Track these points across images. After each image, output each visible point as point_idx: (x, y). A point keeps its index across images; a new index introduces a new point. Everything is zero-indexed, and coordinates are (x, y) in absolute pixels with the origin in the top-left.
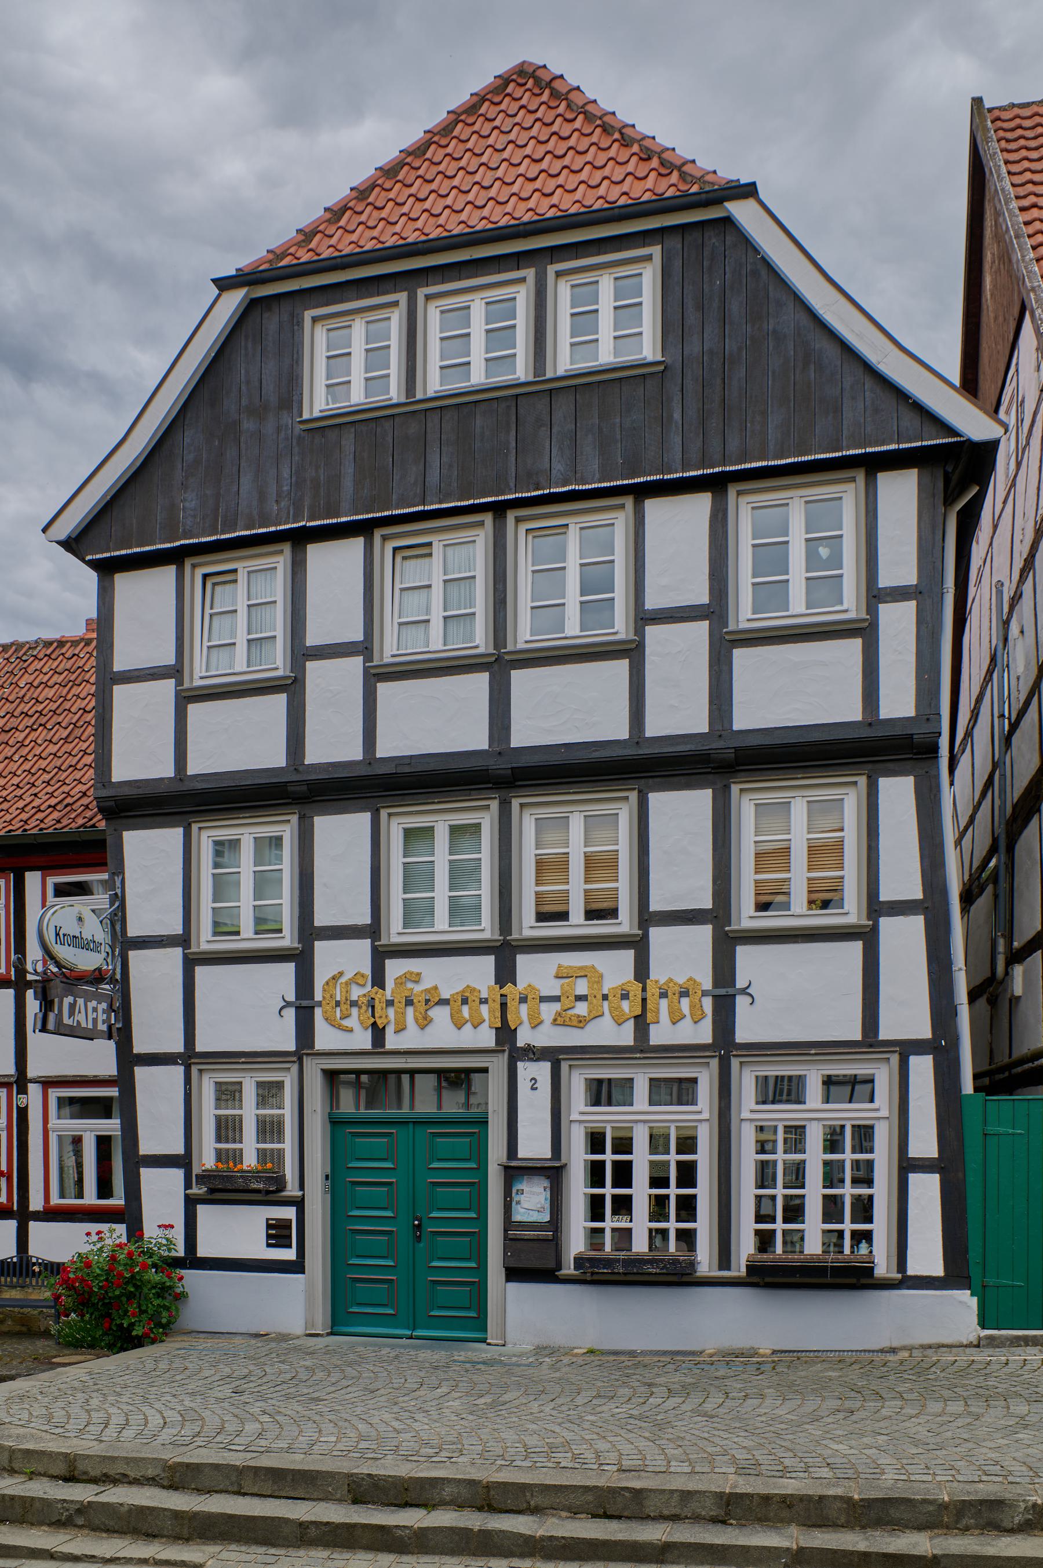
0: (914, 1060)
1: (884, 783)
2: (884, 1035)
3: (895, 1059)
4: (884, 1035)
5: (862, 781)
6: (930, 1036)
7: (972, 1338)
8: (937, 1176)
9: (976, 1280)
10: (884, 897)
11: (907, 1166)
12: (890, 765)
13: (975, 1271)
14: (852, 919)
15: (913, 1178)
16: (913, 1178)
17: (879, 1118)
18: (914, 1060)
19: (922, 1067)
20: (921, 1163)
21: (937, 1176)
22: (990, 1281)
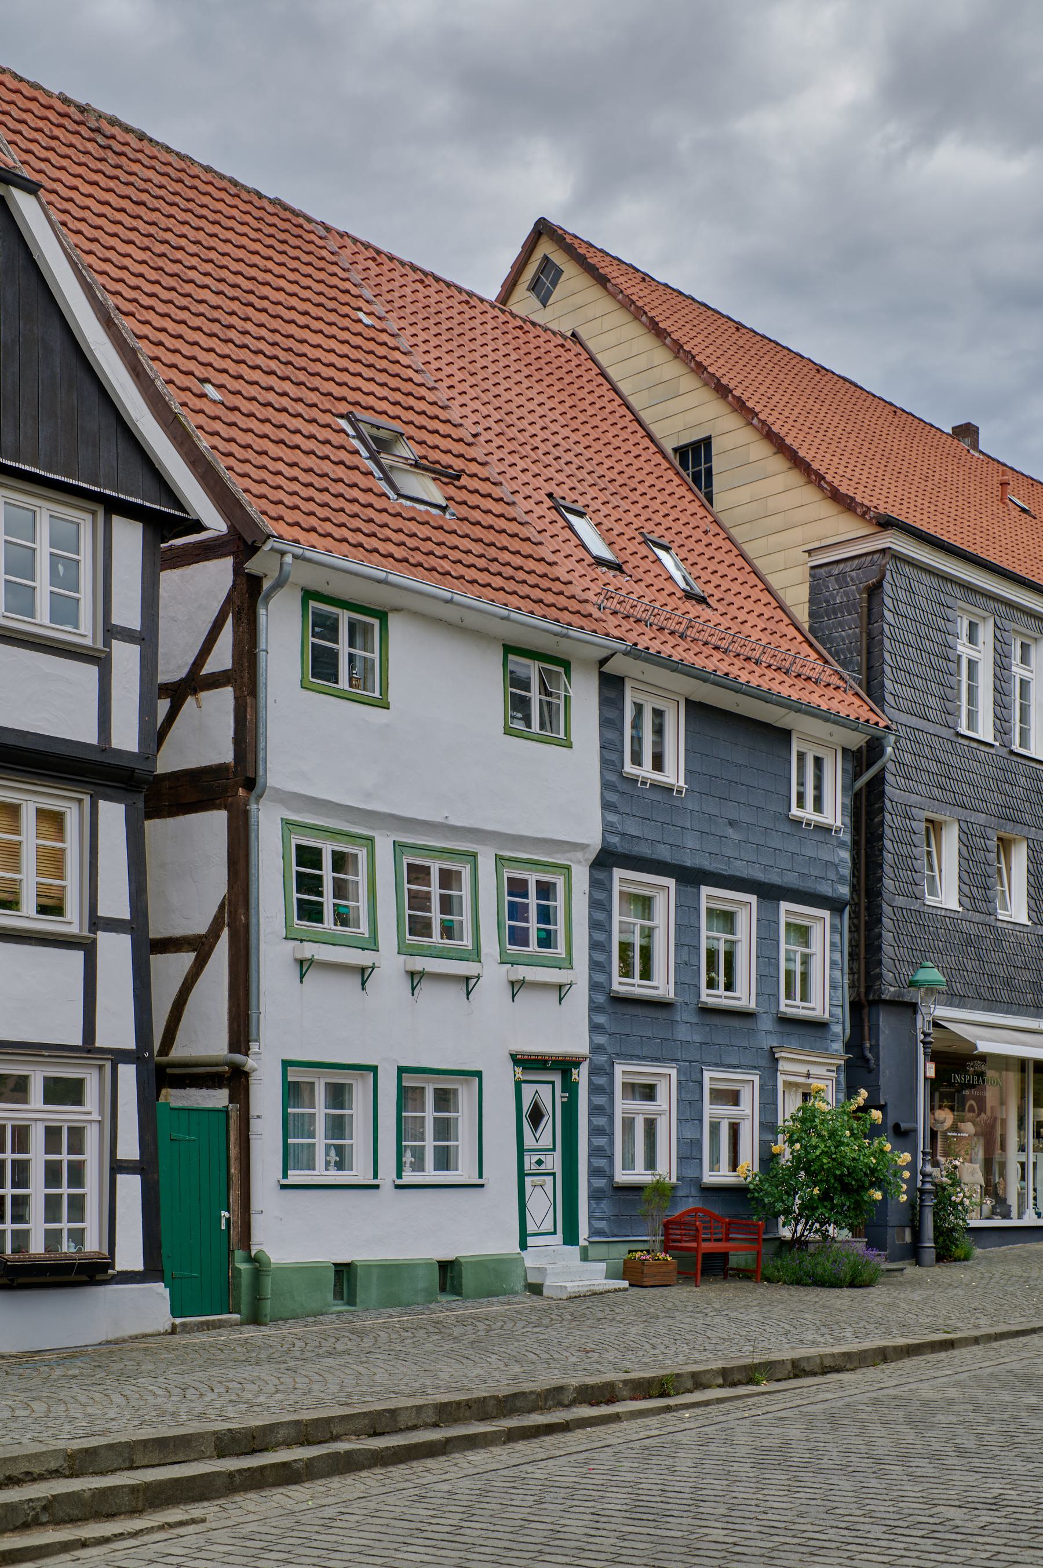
0: (122, 1068)
1: (103, 805)
2: (99, 1043)
3: (108, 1065)
4: (99, 1043)
5: (87, 799)
6: (134, 1047)
7: (168, 1327)
8: (139, 1177)
9: (167, 1275)
10: (101, 912)
11: (117, 1167)
12: (108, 791)
13: (166, 1264)
14: (74, 929)
15: (121, 1178)
16: (121, 1178)
17: (90, 1122)
18: (122, 1068)
19: (128, 1073)
20: (125, 1165)
21: (139, 1177)
22: (177, 1273)
